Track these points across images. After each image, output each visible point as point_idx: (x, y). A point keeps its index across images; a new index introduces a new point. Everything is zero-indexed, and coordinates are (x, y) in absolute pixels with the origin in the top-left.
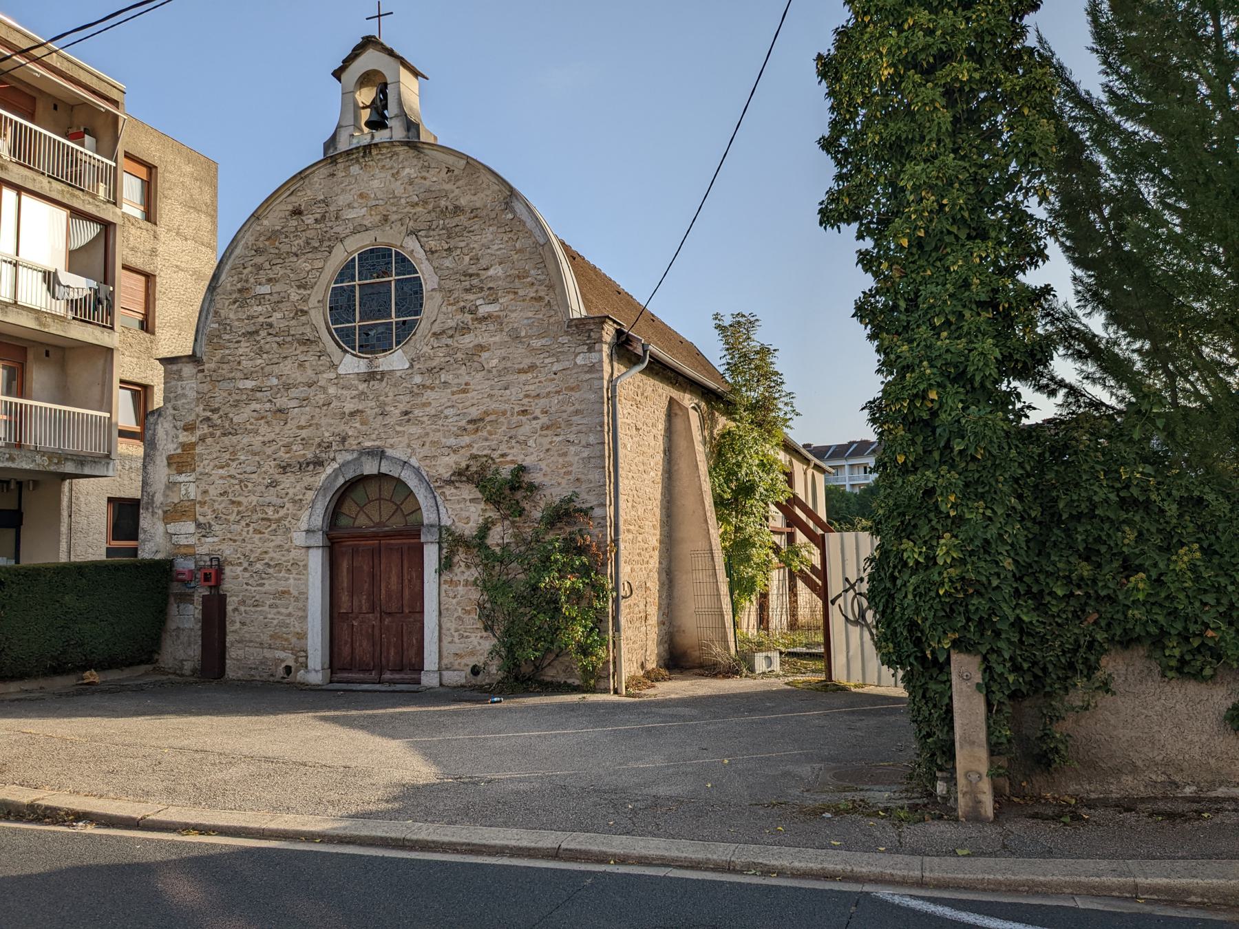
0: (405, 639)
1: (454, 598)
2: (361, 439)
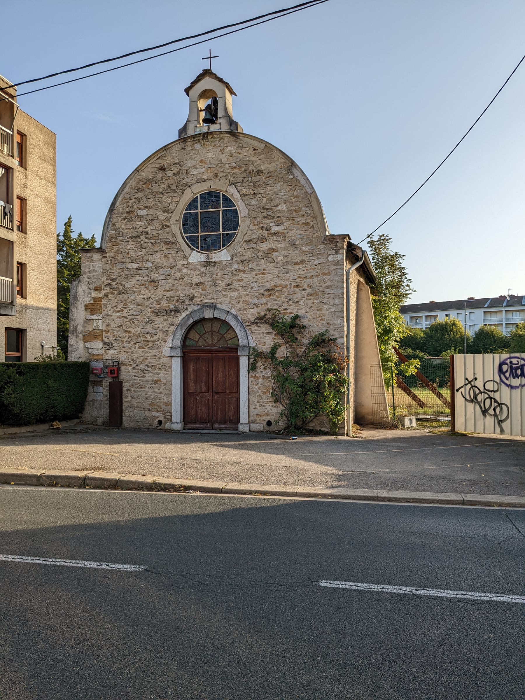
0: (227, 406)
1: (257, 385)
2: (202, 298)
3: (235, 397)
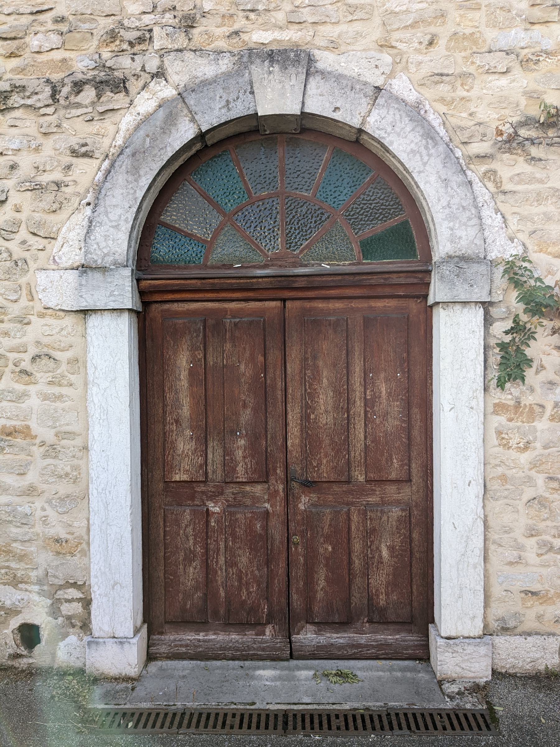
0: (357, 546)
1: (526, 447)
2: (240, 23)
3: (398, 502)
